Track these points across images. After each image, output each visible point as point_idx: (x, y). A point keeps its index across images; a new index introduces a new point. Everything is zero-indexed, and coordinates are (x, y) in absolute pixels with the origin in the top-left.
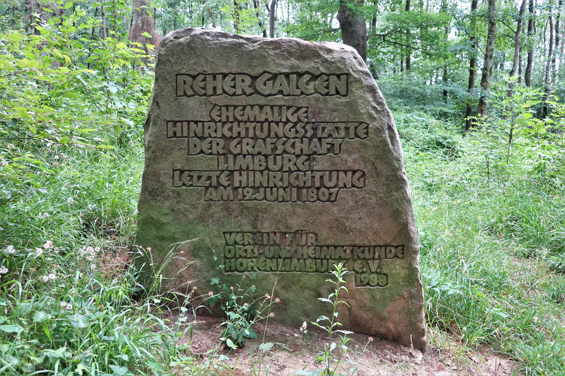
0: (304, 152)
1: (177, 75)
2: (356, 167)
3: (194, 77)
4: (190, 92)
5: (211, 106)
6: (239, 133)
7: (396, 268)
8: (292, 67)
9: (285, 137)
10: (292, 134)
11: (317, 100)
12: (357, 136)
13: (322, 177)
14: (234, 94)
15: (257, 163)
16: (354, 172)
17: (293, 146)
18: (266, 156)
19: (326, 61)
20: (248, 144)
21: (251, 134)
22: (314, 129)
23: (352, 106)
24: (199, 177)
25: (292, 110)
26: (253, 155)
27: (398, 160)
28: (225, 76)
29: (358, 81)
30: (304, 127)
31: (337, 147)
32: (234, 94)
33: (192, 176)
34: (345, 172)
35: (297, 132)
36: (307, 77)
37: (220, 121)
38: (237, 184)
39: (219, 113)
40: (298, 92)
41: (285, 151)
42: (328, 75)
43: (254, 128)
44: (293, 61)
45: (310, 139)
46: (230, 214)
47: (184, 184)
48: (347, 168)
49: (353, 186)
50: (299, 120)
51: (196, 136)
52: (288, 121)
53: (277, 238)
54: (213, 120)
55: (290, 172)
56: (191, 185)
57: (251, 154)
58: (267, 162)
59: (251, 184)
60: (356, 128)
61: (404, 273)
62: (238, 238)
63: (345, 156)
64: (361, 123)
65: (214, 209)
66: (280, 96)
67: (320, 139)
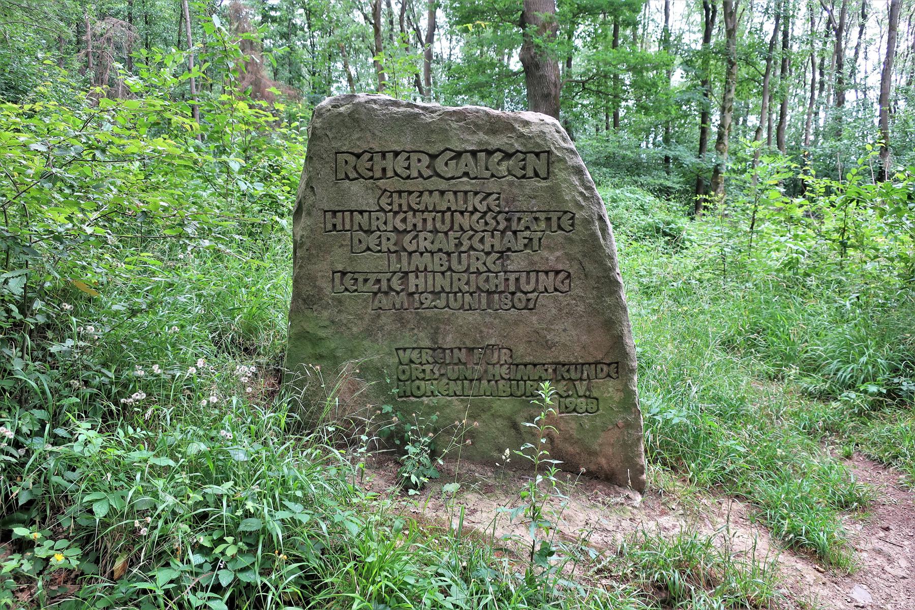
0: (496, 249)
1: (336, 153)
2: (560, 267)
3: (358, 156)
4: (353, 175)
5: (380, 192)
6: (415, 225)
7: (609, 390)
8: (480, 143)
9: (472, 229)
10: (480, 227)
11: (511, 184)
12: (560, 228)
13: (517, 280)
14: (408, 177)
15: (437, 263)
16: (557, 272)
17: (482, 240)
18: (449, 254)
19: (522, 135)
20: (425, 239)
21: (430, 226)
22: (508, 219)
23: (554, 192)
24: (366, 280)
25: (480, 197)
26: (432, 253)
27: (611, 258)
28: (396, 154)
29: (562, 160)
30: (495, 218)
31: (535, 242)
32: (408, 177)
33: (356, 280)
34: (547, 273)
35: (486, 224)
36: (498, 156)
37: (391, 211)
38: (412, 289)
39: (389, 201)
40: (487, 174)
41: (472, 248)
42: (525, 153)
43: (434, 219)
44: (481, 136)
45: (503, 232)
46: (403, 325)
47: (346, 290)
48: (548, 268)
49: (556, 290)
50: (489, 209)
51: (361, 229)
53: (463, 355)
54: (382, 210)
55: (478, 272)
56: (356, 291)
57: (430, 252)
58: (449, 261)
59: (430, 289)
60: (559, 219)
61: (618, 396)
62: (415, 355)
63: (545, 253)
64: (565, 212)
65: (384, 320)
66: (465, 179)
67: (515, 233)
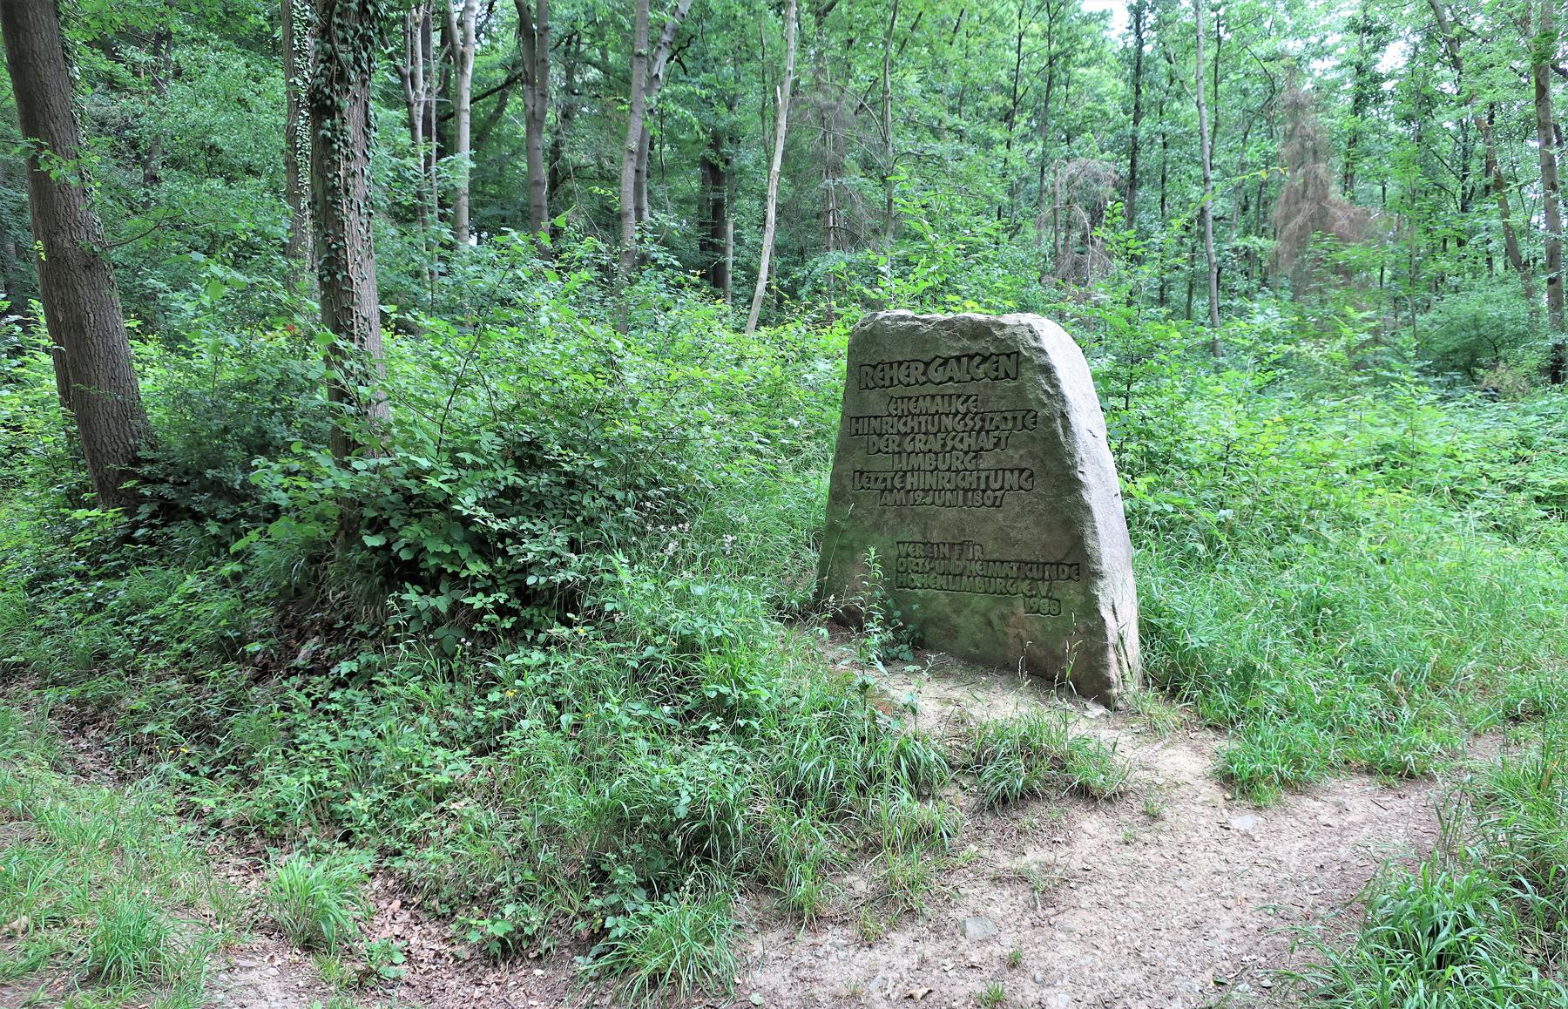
2: (1024, 465)
3: (875, 367)
4: (871, 385)
7: (1070, 592)
8: (963, 349)
10: (960, 428)
11: (986, 385)
12: (1024, 426)
13: (988, 478)
15: (926, 462)
16: (1022, 471)
17: (961, 440)
18: (936, 454)
19: (996, 339)
22: (982, 422)
23: (1020, 392)
27: (1072, 456)
28: (900, 363)
29: (1029, 360)
31: (1003, 441)
34: (1012, 471)
36: (978, 359)
40: (968, 377)
44: (966, 342)
45: (979, 433)
46: (903, 521)
52: (958, 412)
53: (946, 550)
55: (958, 471)
61: (1079, 599)
62: (911, 549)
63: (1011, 452)
65: (888, 515)
